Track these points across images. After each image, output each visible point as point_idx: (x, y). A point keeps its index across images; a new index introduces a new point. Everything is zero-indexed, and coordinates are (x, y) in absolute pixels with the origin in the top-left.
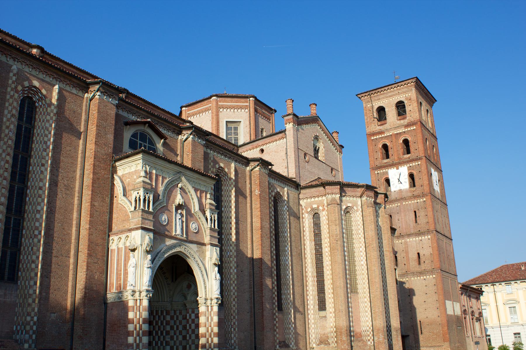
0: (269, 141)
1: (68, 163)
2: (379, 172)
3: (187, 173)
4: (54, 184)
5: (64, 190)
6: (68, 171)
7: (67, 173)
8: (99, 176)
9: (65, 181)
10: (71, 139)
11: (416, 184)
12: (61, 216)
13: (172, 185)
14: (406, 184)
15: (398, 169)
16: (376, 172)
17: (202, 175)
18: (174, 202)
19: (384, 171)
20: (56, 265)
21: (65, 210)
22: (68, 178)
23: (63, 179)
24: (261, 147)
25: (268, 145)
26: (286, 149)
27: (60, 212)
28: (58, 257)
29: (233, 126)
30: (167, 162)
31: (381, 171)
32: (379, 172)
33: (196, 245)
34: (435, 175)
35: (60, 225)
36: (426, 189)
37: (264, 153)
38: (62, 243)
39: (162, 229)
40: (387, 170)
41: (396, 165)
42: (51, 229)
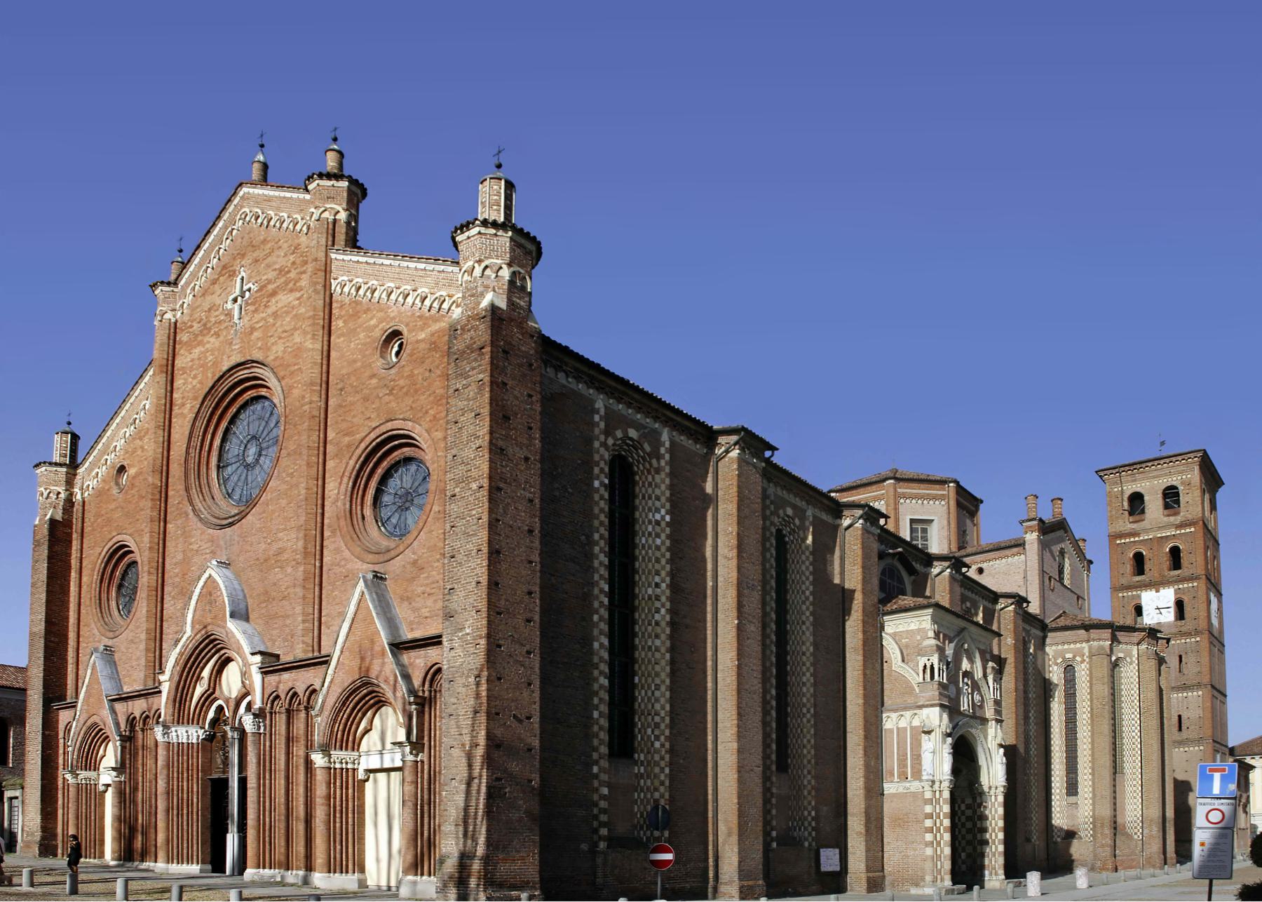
0: (993, 556)
2: (1125, 594)
11: (1187, 615)
14: (1169, 616)
15: (1157, 591)
16: (1121, 595)
19: (1134, 593)
24: (980, 565)
25: (991, 563)
26: (1025, 571)
29: (919, 525)
31: (1130, 593)
32: (1125, 594)
34: (1214, 600)
36: (1203, 624)
37: (984, 574)
40: (1139, 592)
41: (1156, 585)
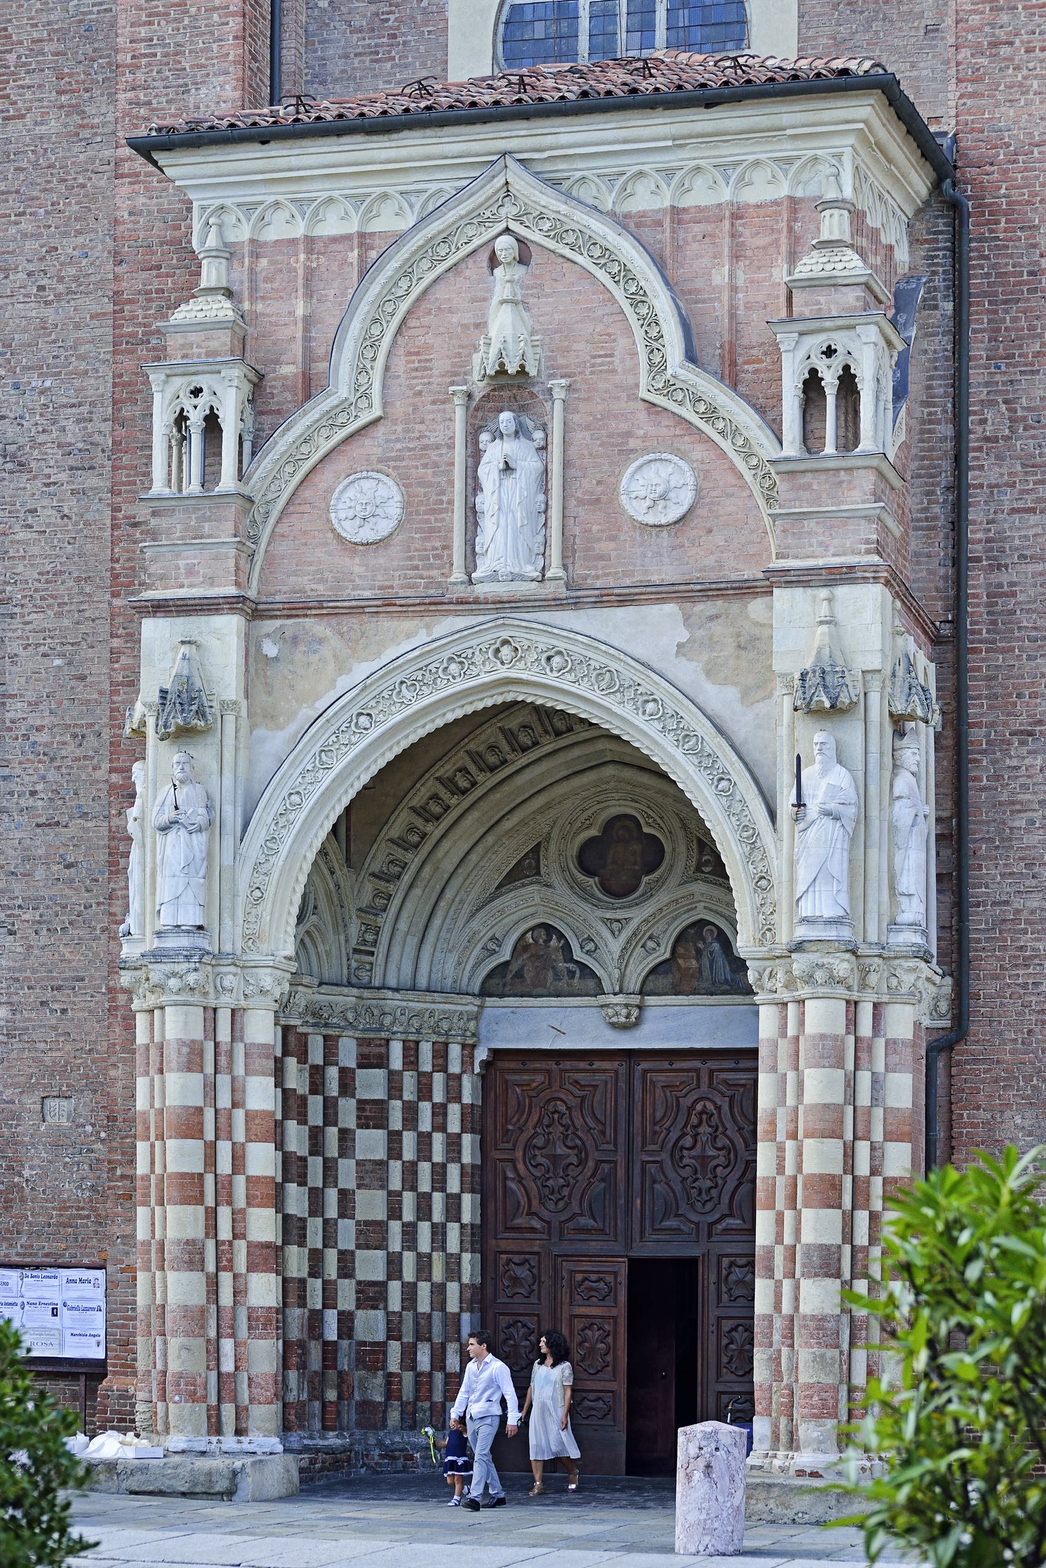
1: (77, 327)
3: (564, 139)
4: (9, 466)
5: (63, 477)
6: (83, 366)
7: (77, 383)
8: (154, 349)
9: (70, 426)
10: (83, 186)
12: (59, 615)
13: (441, 268)
17: (709, 105)
18: (459, 373)
20: (55, 868)
21: (78, 580)
22: (85, 409)
23: (54, 422)
27: (52, 597)
28: (58, 824)
30: (359, 138)
33: (671, 608)
35: (58, 662)
38: (78, 752)
39: (357, 570)
42: (14, 696)
